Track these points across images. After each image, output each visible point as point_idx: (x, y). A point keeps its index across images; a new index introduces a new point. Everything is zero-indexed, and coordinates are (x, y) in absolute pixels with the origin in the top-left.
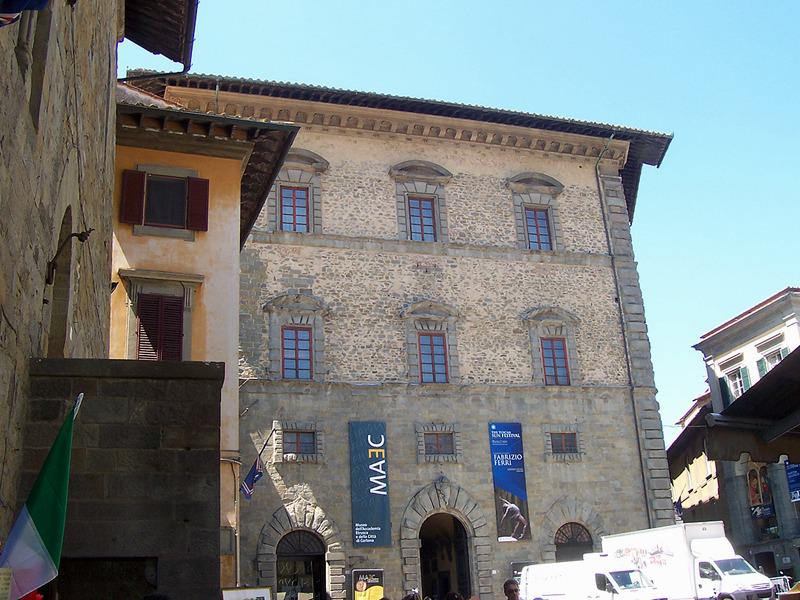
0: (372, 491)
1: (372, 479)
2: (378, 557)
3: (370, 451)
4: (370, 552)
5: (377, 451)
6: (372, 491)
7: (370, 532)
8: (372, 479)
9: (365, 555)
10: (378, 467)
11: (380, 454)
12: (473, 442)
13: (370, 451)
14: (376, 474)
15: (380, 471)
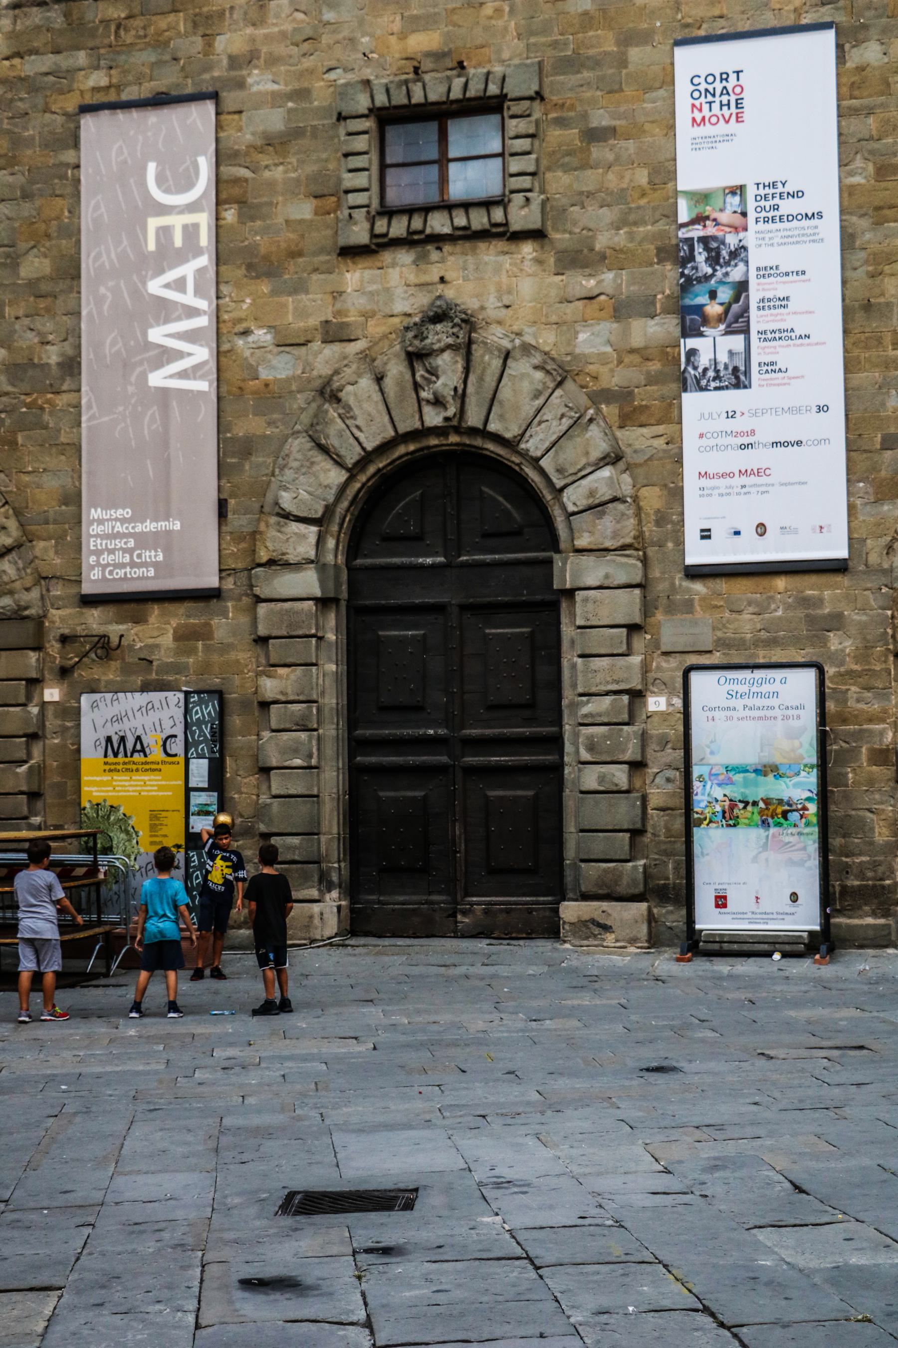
0: (156, 379)
1: (156, 335)
2: (167, 640)
3: (153, 223)
4: (139, 620)
5: (177, 222)
6: (156, 379)
7: (144, 541)
8: (156, 335)
9: (115, 630)
10: (179, 285)
11: (191, 232)
12: (594, 135)
13: (153, 223)
14: (164, 310)
15: (189, 298)
